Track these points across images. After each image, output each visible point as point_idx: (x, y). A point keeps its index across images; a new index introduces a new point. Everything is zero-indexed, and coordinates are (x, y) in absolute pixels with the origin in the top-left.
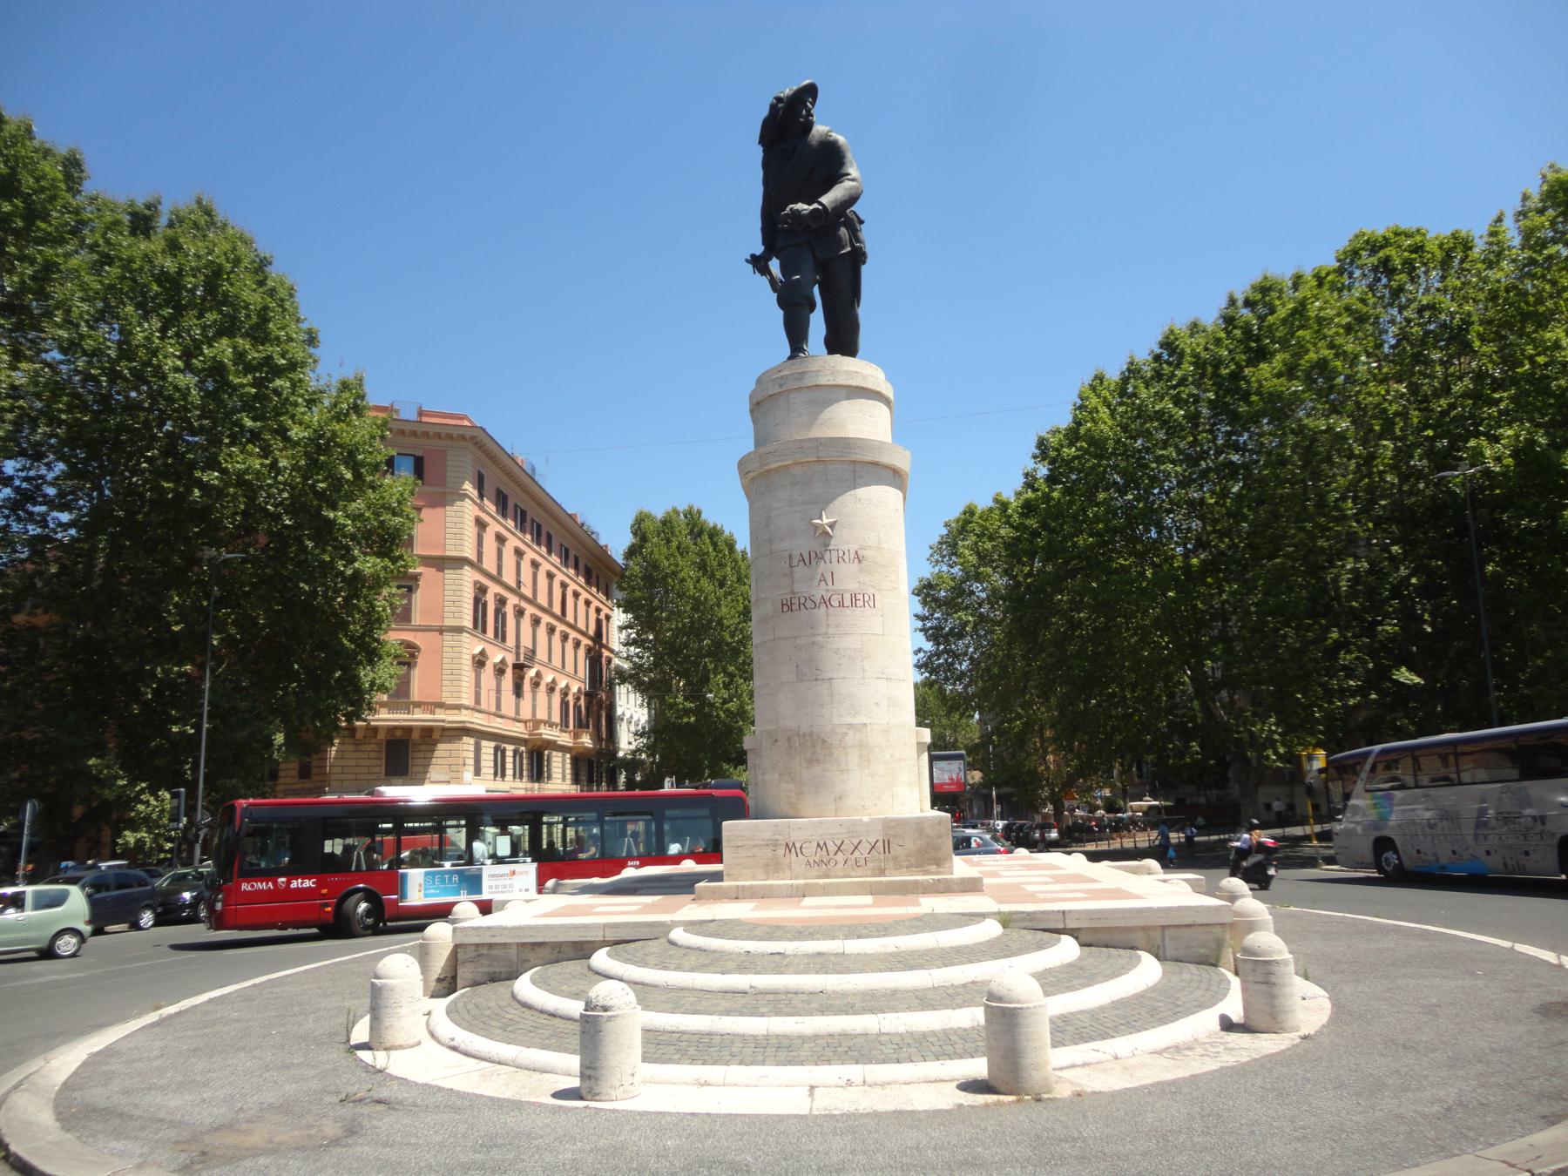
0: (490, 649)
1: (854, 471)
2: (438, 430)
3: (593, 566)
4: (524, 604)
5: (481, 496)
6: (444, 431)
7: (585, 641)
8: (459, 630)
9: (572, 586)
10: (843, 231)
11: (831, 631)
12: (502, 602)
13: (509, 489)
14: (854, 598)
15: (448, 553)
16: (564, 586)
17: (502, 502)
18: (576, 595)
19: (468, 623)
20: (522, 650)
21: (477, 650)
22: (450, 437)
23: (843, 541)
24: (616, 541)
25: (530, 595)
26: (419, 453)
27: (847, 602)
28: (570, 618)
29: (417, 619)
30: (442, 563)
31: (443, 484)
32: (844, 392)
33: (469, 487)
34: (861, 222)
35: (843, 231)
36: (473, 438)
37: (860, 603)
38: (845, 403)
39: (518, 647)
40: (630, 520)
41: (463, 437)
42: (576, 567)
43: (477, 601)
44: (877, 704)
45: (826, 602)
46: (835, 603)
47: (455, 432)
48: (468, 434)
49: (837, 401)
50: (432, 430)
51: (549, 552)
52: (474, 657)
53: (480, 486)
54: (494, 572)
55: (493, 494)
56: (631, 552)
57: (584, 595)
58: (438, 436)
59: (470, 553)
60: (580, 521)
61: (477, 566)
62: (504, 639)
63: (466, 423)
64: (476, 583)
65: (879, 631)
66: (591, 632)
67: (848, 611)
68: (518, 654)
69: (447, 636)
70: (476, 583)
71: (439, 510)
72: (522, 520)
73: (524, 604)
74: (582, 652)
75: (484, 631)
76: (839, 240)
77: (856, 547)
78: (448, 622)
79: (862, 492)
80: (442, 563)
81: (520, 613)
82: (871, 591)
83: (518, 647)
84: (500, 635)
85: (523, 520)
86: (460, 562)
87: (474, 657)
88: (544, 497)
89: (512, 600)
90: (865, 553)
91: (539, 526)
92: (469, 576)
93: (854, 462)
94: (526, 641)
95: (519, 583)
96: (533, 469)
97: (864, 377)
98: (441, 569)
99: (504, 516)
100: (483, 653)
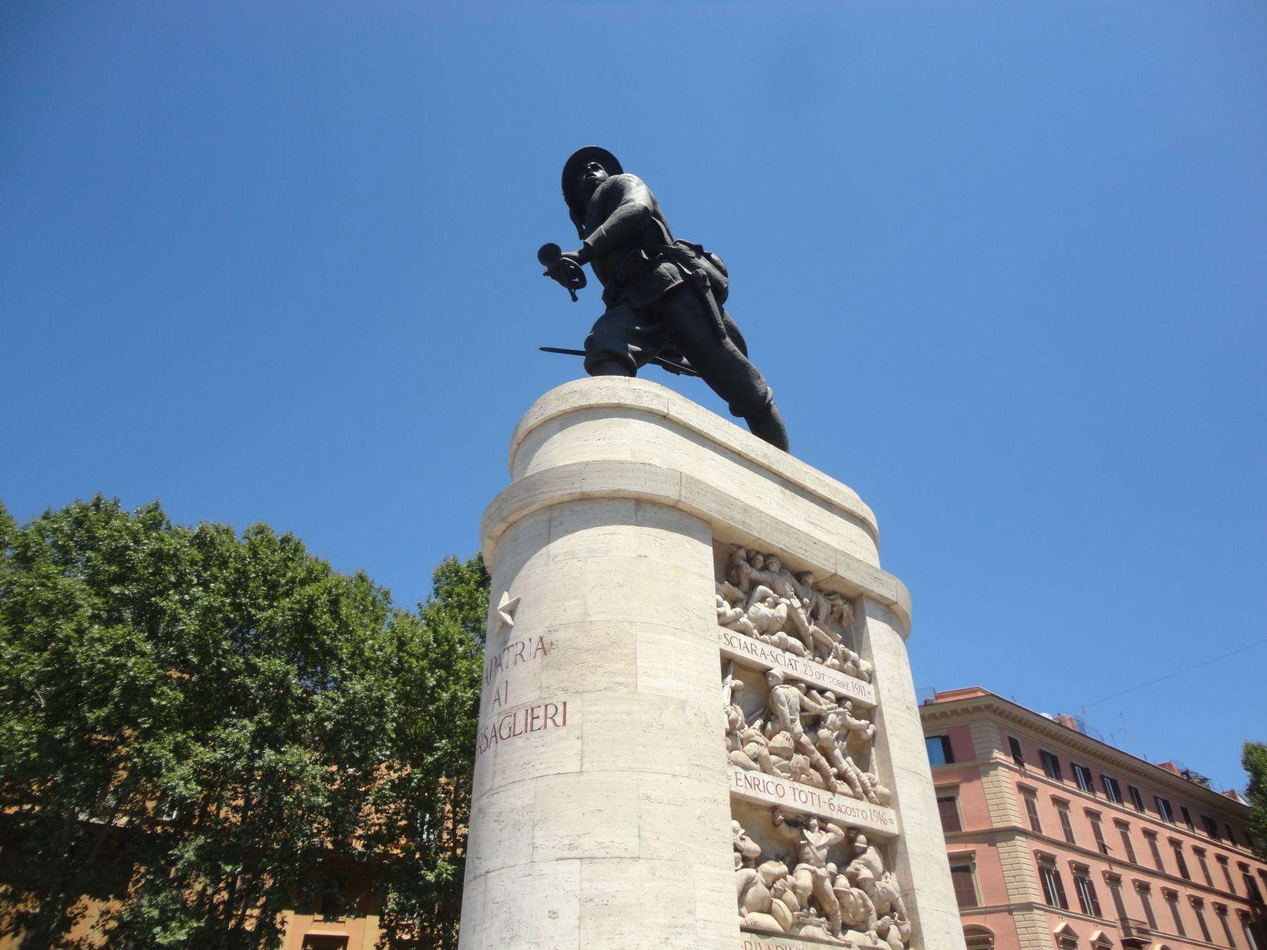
0: (1076, 926)
1: (550, 520)
2: (953, 707)
3: (1216, 817)
4: (1117, 870)
5: (1019, 762)
6: (958, 707)
7: (1232, 906)
8: (1029, 907)
9: (1188, 844)
10: (666, 267)
11: (499, 780)
12: (1081, 873)
13: (1053, 748)
14: (531, 713)
15: (996, 826)
16: (1175, 844)
17: (1052, 766)
18: (1199, 852)
19: (1037, 897)
20: (1131, 924)
21: (1058, 929)
22: (966, 711)
23: (526, 629)
24: (1231, 781)
25: (1125, 859)
26: (944, 733)
27: (520, 728)
28: (1197, 876)
29: (982, 901)
30: (993, 837)
31: (973, 757)
32: (556, 424)
33: (998, 755)
34: (699, 250)
35: (666, 267)
36: (988, 707)
37: (538, 723)
38: (558, 437)
39: (1124, 919)
40: (1239, 755)
41: (977, 709)
42: (1188, 820)
43: (1042, 871)
44: (553, 915)
45: (496, 735)
46: (505, 733)
47: (969, 706)
48: (981, 704)
49: (545, 440)
50: (948, 709)
51: (1140, 807)
52: (1057, 936)
53: (1015, 750)
54: (1063, 839)
55: (1037, 757)
56: (1253, 790)
57: (1211, 851)
58: (955, 713)
59: (1018, 818)
60: (1177, 770)
61: (1035, 833)
62: (1098, 912)
63: (980, 694)
64: (1036, 852)
65: (573, 766)
66: (1242, 891)
67: (519, 741)
68: (1126, 929)
69: (1018, 916)
70: (1036, 852)
71: (976, 783)
72: (1087, 780)
73: (1117, 870)
74: (1234, 921)
75: (1064, 905)
76: (661, 276)
77: (540, 631)
78: (1015, 900)
79: (559, 546)
80: (993, 837)
81: (1114, 881)
82: (559, 699)
83: (1124, 919)
84: (1092, 907)
85: (1088, 778)
86: (1010, 833)
87: (1057, 936)
88: (1117, 755)
89: (1097, 870)
90: (554, 637)
91: (1114, 783)
92: (1024, 849)
93: (551, 507)
94: (1135, 911)
95: (1103, 847)
96: (1082, 724)
97: (583, 394)
98: (992, 843)
99: (1059, 778)
100: (1067, 930)
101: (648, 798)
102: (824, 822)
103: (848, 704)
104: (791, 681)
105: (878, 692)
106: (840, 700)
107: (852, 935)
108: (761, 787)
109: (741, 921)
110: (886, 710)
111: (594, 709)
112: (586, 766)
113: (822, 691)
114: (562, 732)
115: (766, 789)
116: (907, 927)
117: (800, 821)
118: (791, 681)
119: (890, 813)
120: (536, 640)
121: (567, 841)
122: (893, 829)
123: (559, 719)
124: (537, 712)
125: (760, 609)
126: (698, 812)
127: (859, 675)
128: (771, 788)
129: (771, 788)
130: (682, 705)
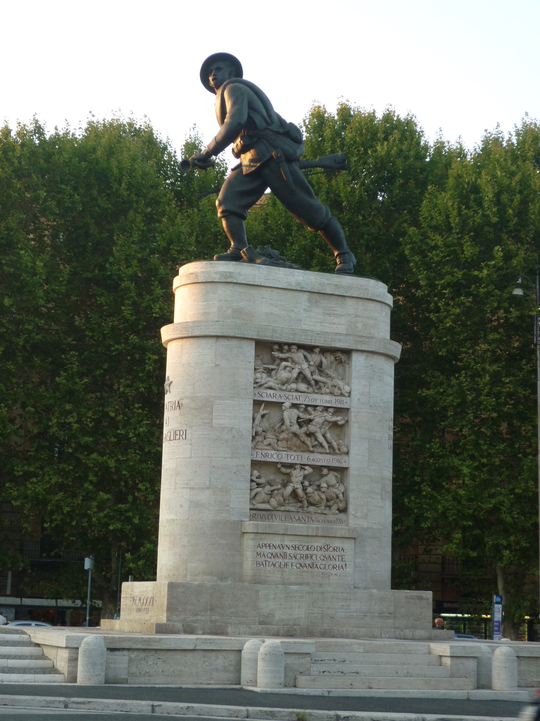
37: (178, 437)
67: (172, 442)
101: (214, 467)
102: (303, 466)
103: (331, 410)
104: (294, 406)
105: (351, 402)
106: (326, 408)
107: (312, 509)
108: (270, 456)
109: (252, 507)
110: (352, 410)
111: (196, 433)
112: (193, 455)
113: (315, 407)
114: (185, 441)
115: (272, 456)
116: (342, 505)
117: (291, 466)
118: (294, 406)
119: (345, 458)
120: (177, 402)
121: (186, 482)
122: (344, 465)
123: (184, 438)
124: (178, 433)
125: (284, 375)
126: (235, 470)
127: (342, 395)
128: (275, 456)
129: (275, 456)
130: (232, 429)
